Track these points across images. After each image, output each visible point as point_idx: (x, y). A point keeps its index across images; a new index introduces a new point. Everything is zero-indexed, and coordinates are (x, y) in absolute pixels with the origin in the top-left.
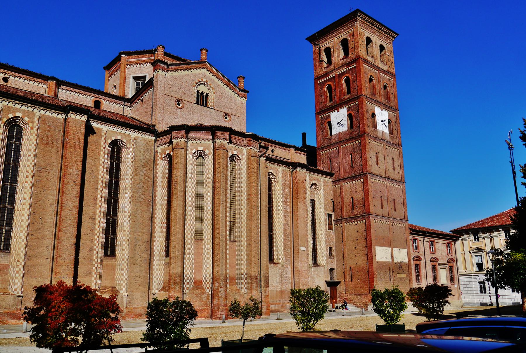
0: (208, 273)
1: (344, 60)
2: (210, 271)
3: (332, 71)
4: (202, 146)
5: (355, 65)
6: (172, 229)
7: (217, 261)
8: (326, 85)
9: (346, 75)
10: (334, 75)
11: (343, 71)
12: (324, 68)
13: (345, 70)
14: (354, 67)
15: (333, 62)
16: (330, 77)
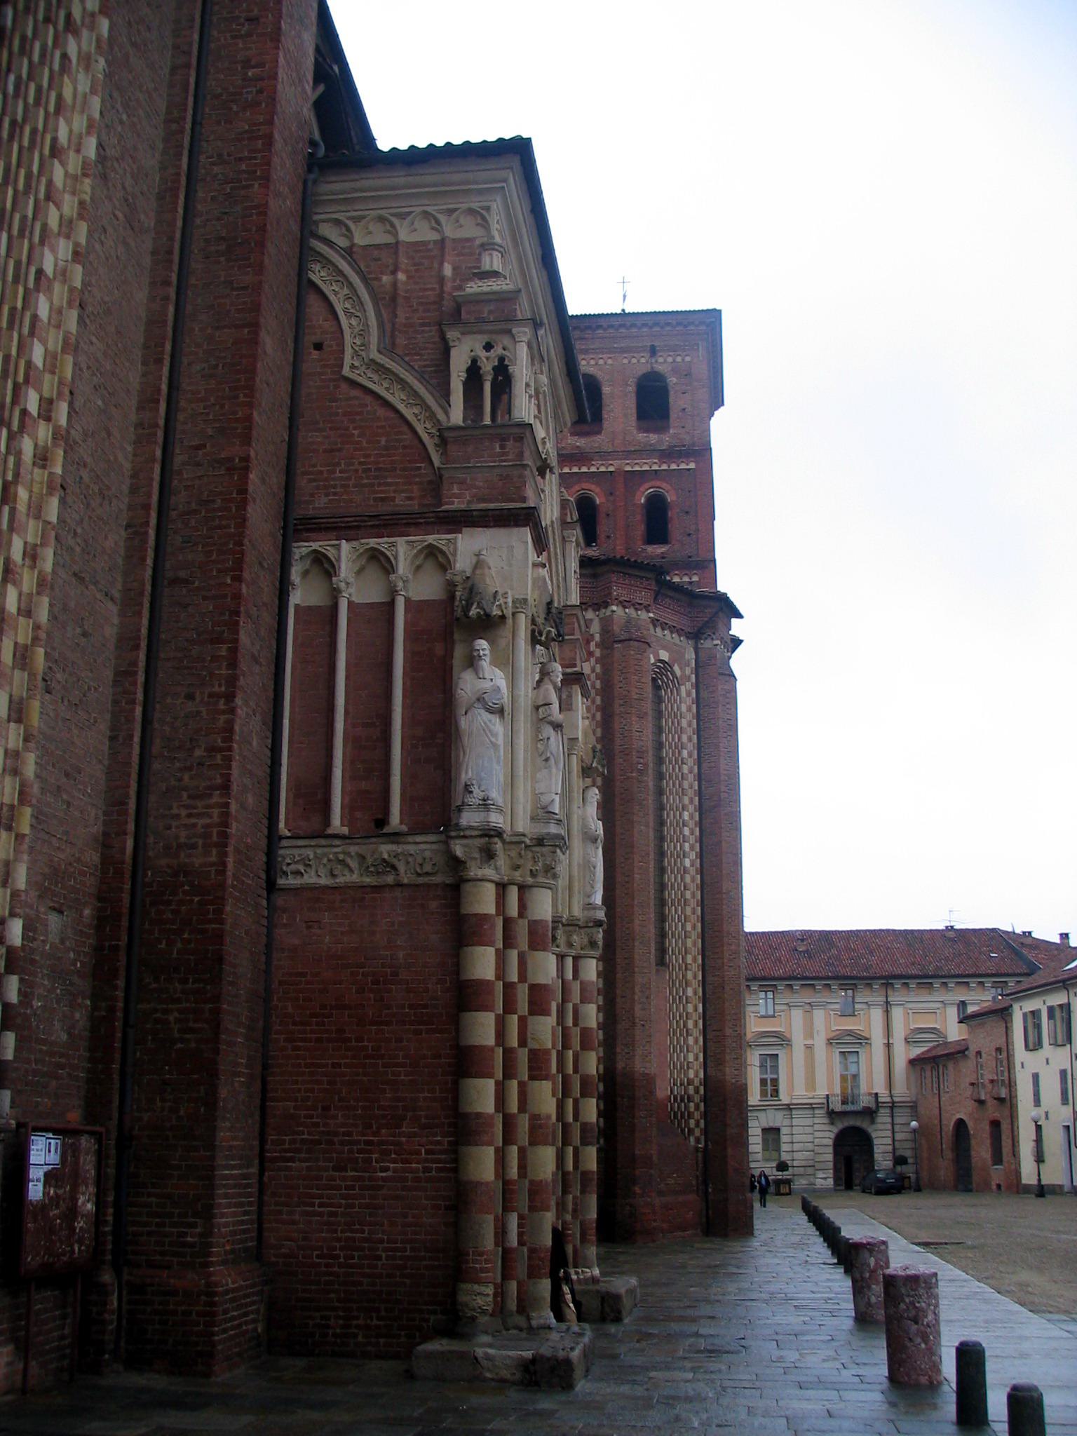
0: (690, 1082)
1: (651, 435)
2: (695, 1073)
3: (604, 455)
4: (664, 648)
5: (692, 466)
6: (637, 922)
7: (734, 1045)
8: (577, 487)
9: (658, 483)
10: (611, 469)
11: (646, 468)
12: (573, 434)
13: (655, 467)
14: (689, 470)
15: (606, 424)
16: (593, 469)
